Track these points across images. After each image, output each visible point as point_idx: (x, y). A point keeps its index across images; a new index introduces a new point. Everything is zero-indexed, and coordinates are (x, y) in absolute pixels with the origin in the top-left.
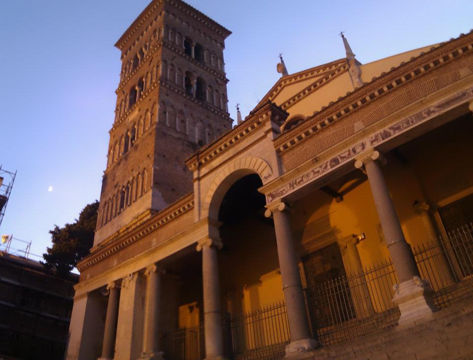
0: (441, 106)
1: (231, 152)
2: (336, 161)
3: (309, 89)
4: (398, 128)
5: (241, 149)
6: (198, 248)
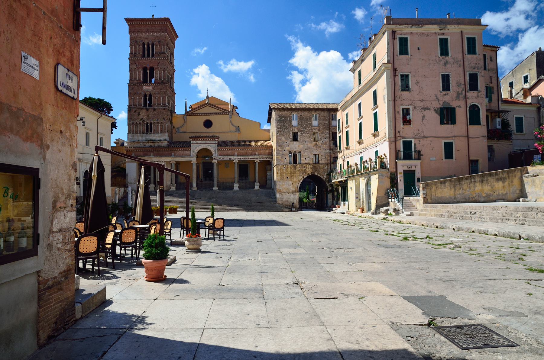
0: (251, 159)
1: (204, 142)
2: (230, 159)
3: (216, 113)
4: (243, 159)
5: (207, 143)
6: (192, 162)
